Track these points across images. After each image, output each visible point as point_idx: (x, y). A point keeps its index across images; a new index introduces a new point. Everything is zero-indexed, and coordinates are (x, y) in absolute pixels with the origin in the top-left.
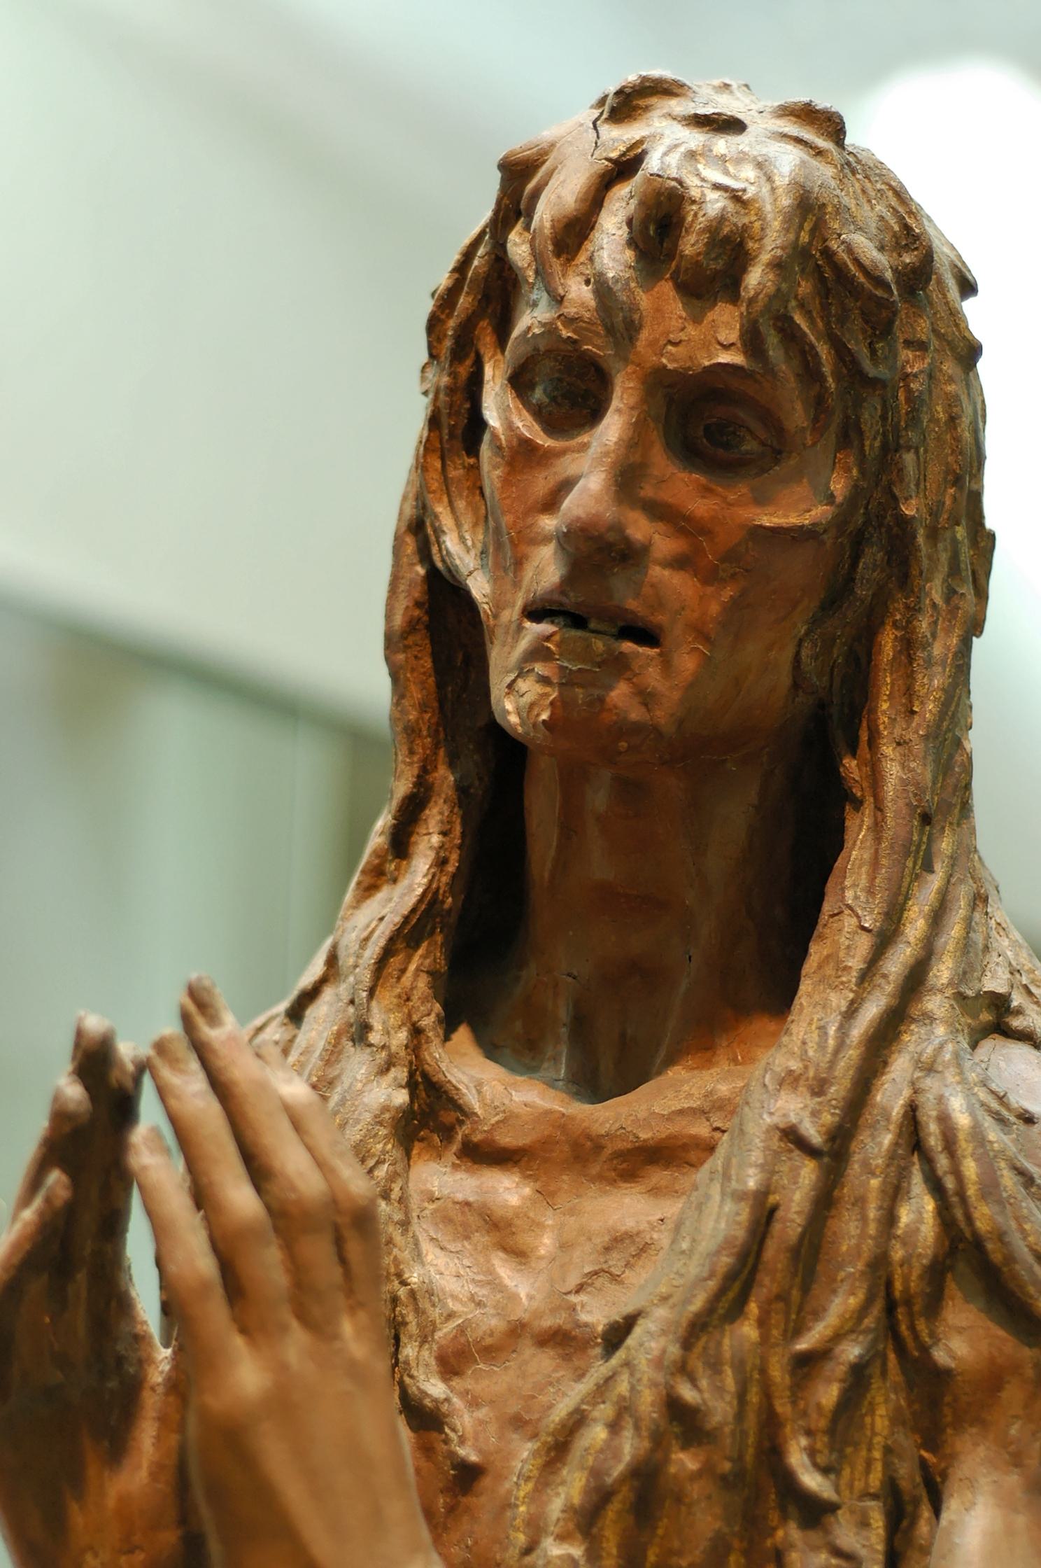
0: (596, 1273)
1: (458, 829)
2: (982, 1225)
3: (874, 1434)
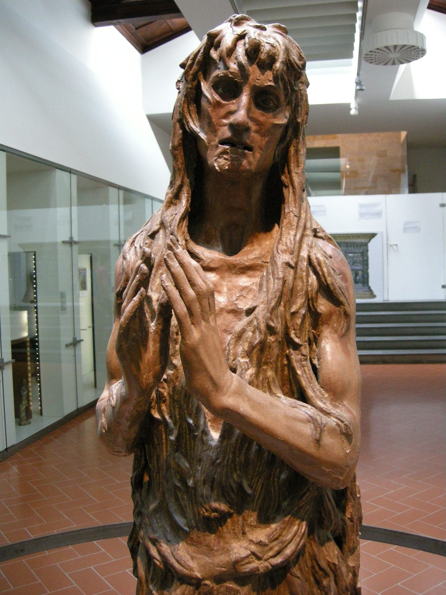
0: (240, 296)
1: (190, 192)
2: (329, 282)
3: (306, 328)
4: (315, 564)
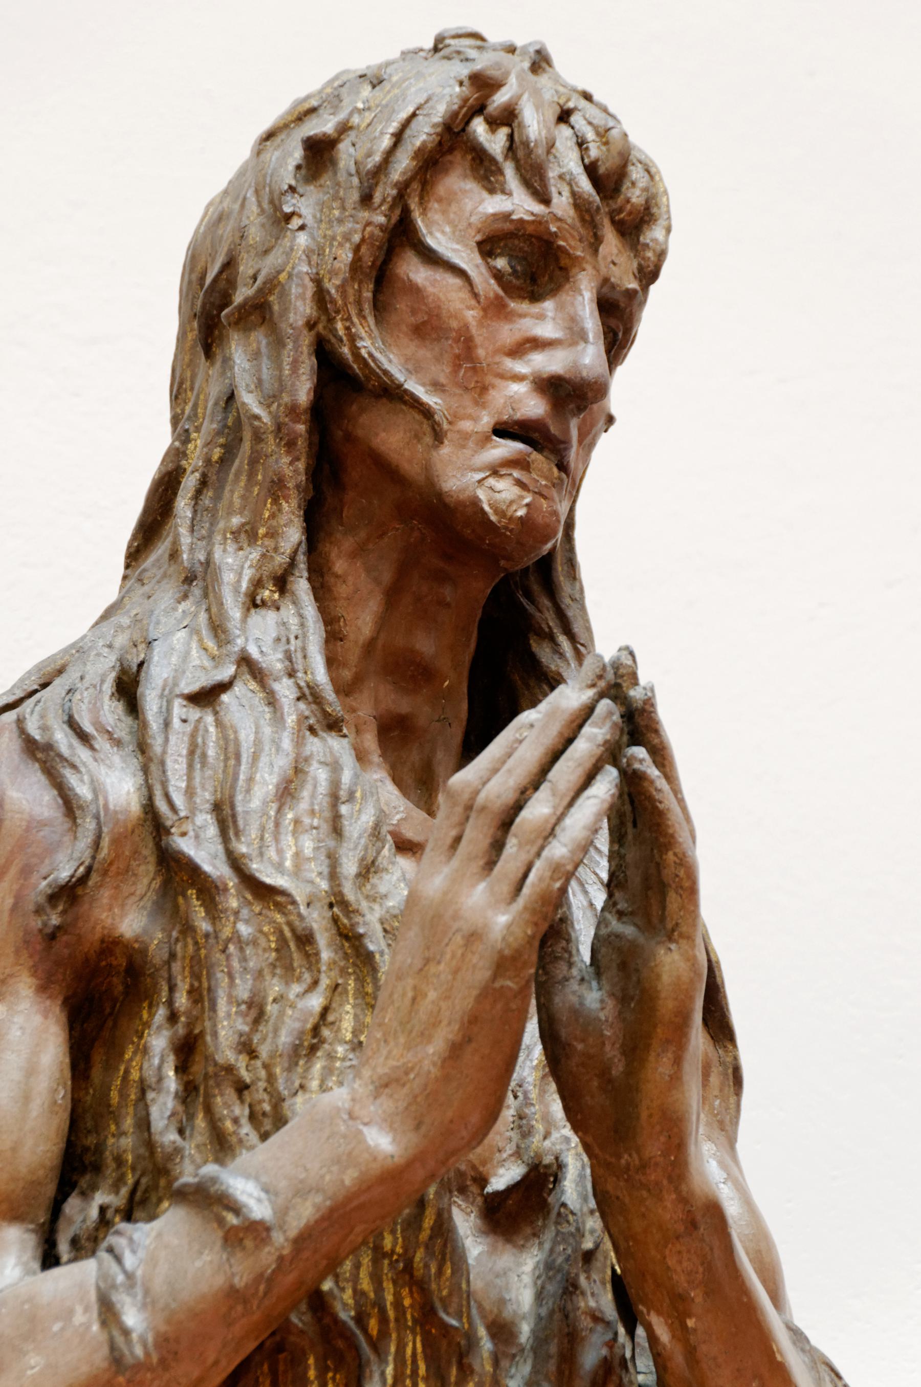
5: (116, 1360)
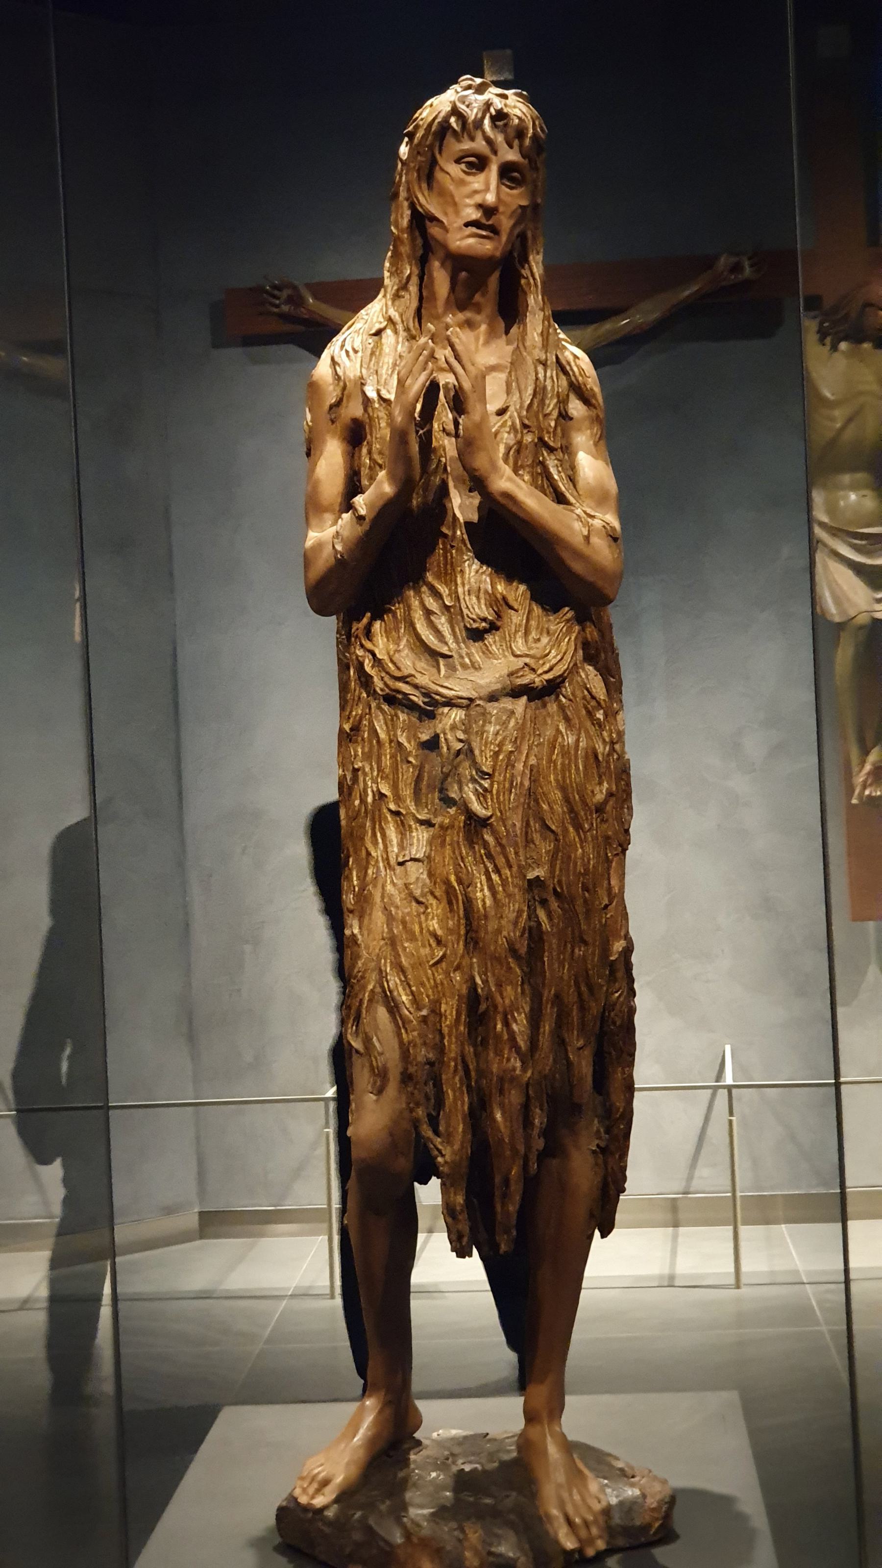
2: (580, 382)
4: (586, 693)
5: (336, 558)
